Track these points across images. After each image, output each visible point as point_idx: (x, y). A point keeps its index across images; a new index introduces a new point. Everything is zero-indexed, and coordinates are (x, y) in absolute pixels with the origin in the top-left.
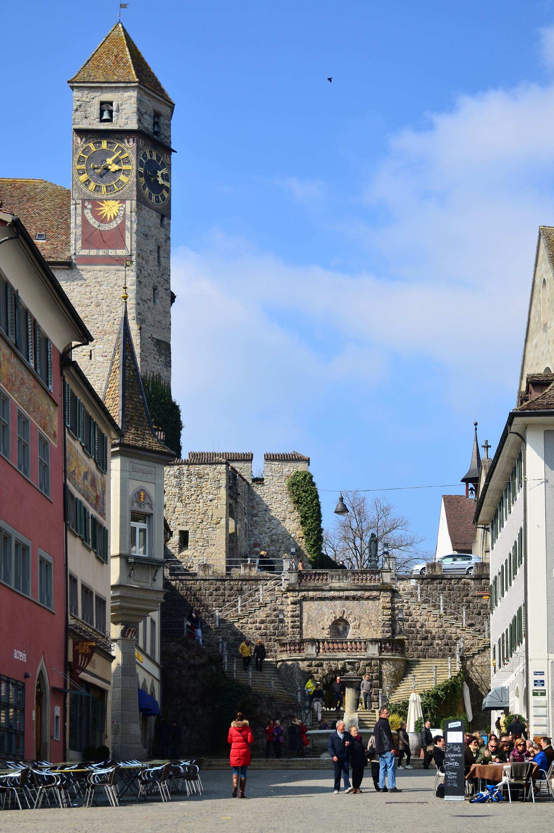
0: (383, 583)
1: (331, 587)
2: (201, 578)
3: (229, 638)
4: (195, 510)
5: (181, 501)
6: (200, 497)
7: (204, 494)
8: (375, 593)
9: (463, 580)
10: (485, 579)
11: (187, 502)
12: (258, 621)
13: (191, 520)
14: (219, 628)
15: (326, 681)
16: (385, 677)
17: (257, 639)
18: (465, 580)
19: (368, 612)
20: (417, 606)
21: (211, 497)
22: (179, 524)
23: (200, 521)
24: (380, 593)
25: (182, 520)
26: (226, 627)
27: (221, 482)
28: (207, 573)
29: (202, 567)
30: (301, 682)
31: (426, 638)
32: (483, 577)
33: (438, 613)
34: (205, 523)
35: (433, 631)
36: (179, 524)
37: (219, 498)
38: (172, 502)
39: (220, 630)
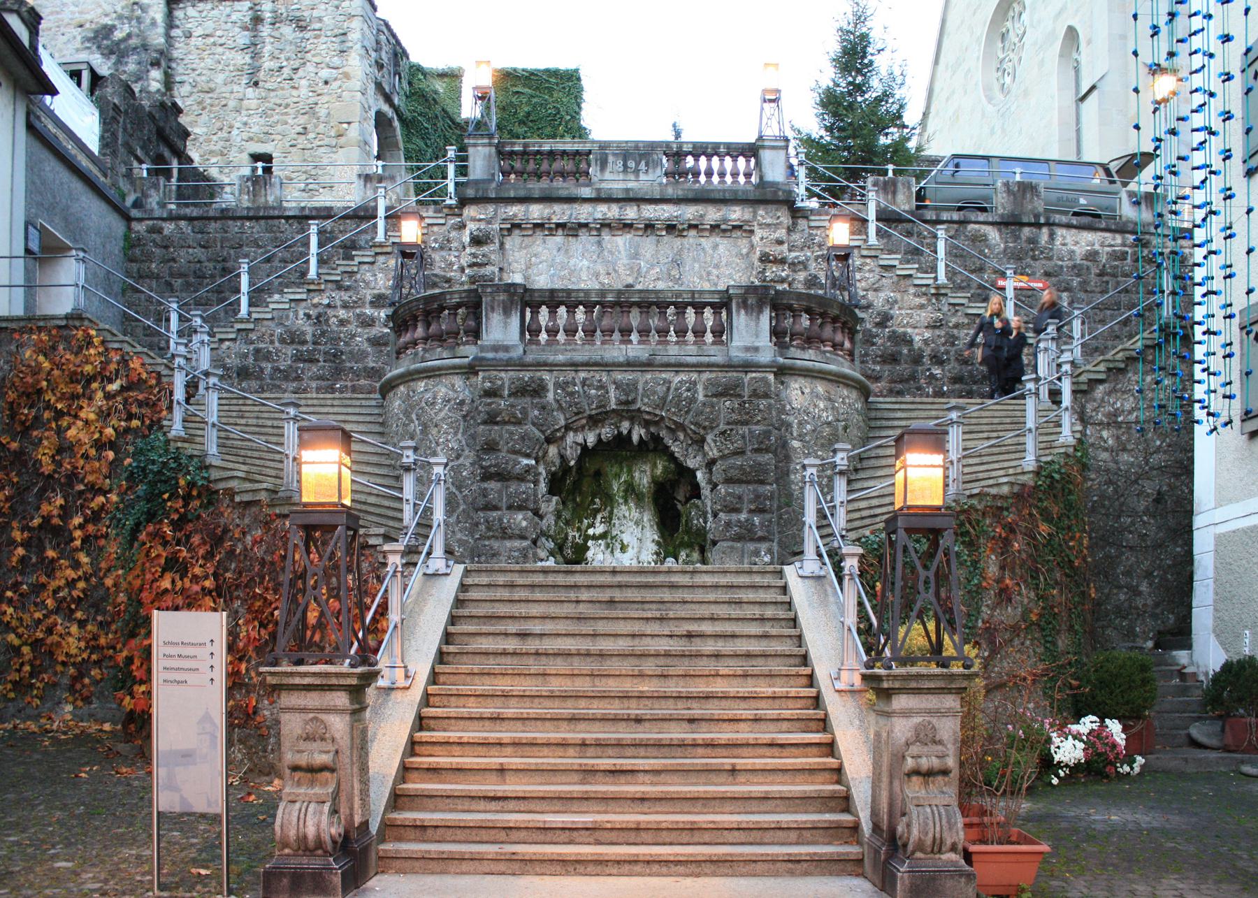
0: (762, 183)
1: (598, 190)
2: (245, 213)
3: (278, 351)
4: (287, 106)
5: (256, 84)
6: (301, 73)
7: (310, 68)
8: (736, 214)
9: (971, 227)
10: (1029, 225)
11: (268, 85)
12: (369, 298)
13: (279, 128)
14: (248, 321)
15: (562, 457)
16: (796, 444)
17: (363, 355)
18: (977, 226)
19: (715, 272)
20: (868, 261)
21: (325, 73)
22: (251, 139)
23: (299, 129)
24: (755, 213)
25: (255, 129)
26: (269, 316)
27: (351, 36)
28: (263, 200)
29: (249, 184)
30: (458, 458)
31: (893, 359)
32: (1025, 220)
33: (931, 282)
34: (311, 136)
35: (917, 338)
36: (251, 139)
37: (347, 76)
38: (236, 88)
39: (251, 326)
